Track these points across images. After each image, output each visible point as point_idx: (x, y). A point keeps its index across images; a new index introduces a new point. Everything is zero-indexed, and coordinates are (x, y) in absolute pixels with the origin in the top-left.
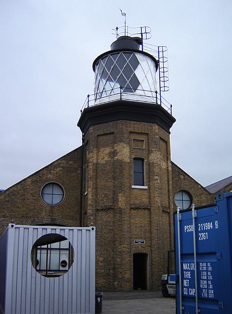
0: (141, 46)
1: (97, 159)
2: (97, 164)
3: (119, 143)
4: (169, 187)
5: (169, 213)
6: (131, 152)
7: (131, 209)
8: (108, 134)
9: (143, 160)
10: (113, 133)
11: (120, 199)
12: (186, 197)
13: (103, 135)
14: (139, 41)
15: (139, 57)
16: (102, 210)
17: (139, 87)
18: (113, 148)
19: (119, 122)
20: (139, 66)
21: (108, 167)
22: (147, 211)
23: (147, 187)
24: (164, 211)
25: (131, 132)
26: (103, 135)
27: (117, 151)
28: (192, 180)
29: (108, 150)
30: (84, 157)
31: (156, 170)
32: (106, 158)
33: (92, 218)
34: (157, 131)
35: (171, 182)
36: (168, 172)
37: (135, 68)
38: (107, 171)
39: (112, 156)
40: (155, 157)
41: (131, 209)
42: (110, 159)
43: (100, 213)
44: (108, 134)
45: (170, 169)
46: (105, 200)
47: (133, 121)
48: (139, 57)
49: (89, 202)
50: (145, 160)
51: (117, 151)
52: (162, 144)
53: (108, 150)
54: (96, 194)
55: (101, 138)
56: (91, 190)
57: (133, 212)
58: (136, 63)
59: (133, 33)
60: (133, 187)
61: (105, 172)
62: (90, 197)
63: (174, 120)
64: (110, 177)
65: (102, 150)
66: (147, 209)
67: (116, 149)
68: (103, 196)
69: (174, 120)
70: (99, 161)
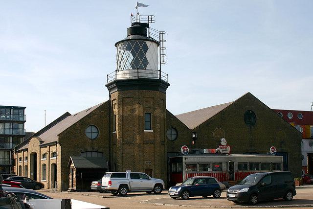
0: (148, 28)
5: (164, 145)
6: (144, 110)
9: (150, 114)
12: (174, 132)
14: (147, 25)
15: (148, 43)
29: (129, 108)
31: (158, 120)
32: (128, 113)
40: (158, 112)
45: (165, 117)
48: (148, 43)
50: (152, 114)
52: (162, 102)
53: (129, 108)
55: (125, 99)
57: (145, 145)
58: (146, 48)
59: (143, 21)
60: (145, 131)
63: (169, 85)
69: (169, 85)
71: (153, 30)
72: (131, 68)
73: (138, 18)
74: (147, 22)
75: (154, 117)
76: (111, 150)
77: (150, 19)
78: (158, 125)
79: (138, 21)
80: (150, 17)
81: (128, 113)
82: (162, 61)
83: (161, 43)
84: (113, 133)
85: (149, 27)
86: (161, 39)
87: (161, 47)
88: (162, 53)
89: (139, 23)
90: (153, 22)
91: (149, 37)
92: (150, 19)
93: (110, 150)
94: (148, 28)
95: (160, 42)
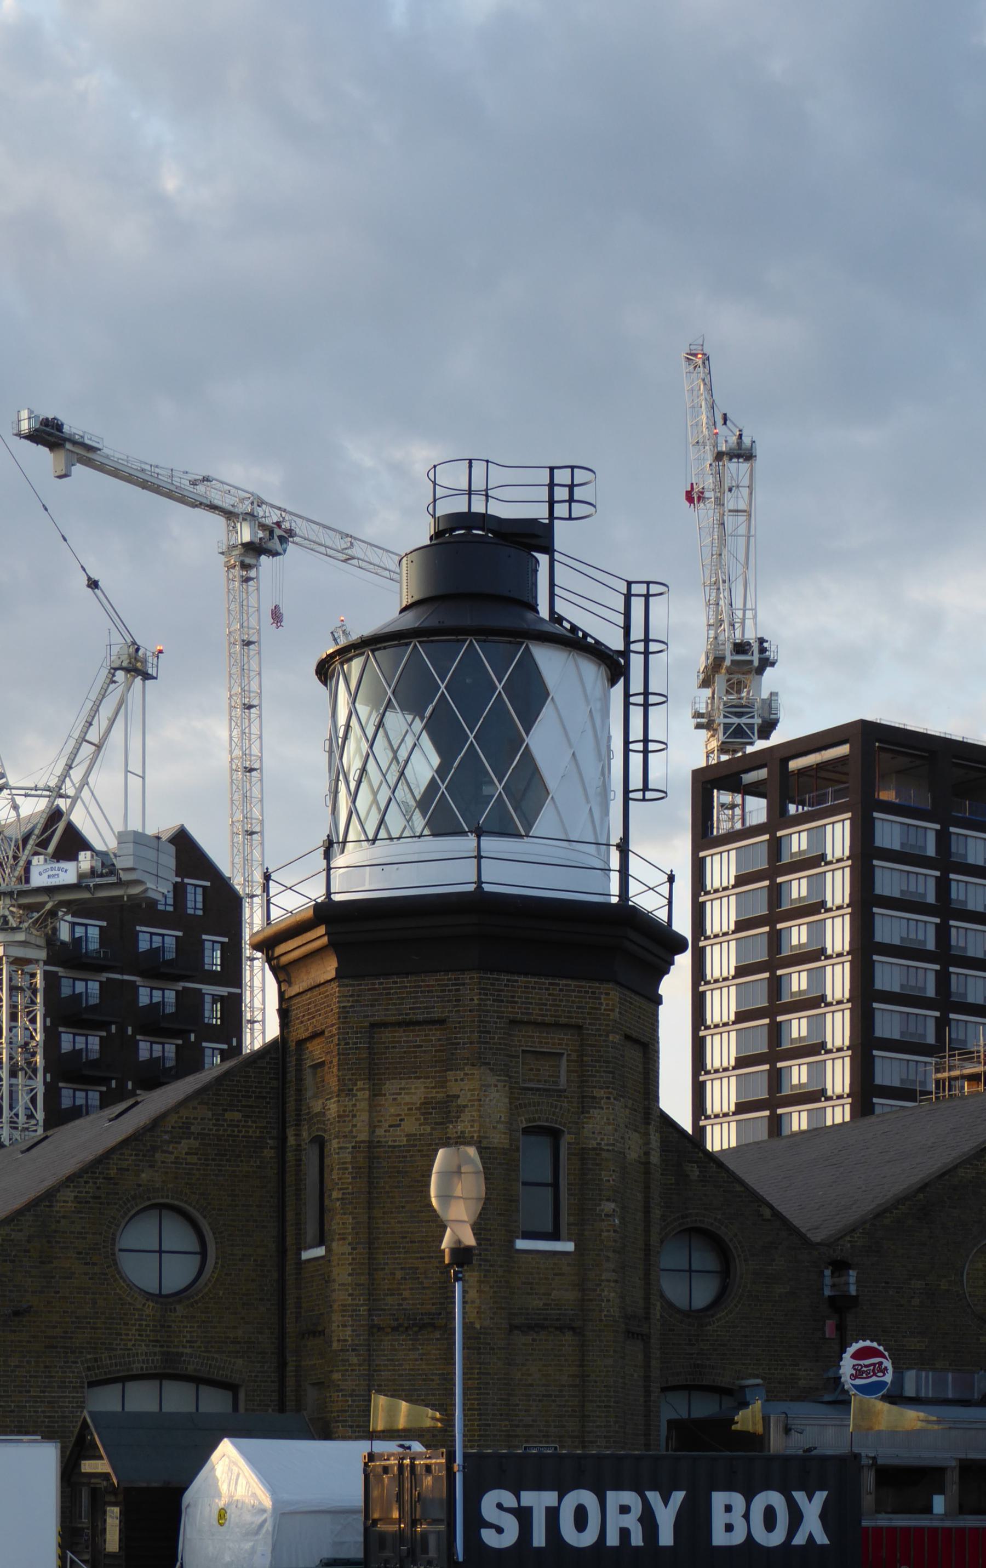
0: (543, 559)
1: (373, 1127)
2: (372, 1145)
3: (467, 1069)
4: (647, 1231)
5: (645, 1338)
7: (512, 1328)
8: (418, 1023)
9: (554, 1134)
10: (442, 1022)
13: (399, 1024)
17: (545, 823)
18: (443, 1084)
19: (466, 977)
20: (547, 712)
22: (568, 1337)
23: (569, 1246)
24: (630, 1334)
25: (513, 1022)
26: (399, 1024)
27: (460, 1102)
28: (739, 1188)
30: (291, 1092)
33: (354, 1360)
34: (615, 1015)
35: (656, 1213)
36: (647, 1173)
37: (530, 720)
41: (512, 1328)
42: (428, 1129)
44: (418, 1023)
45: (655, 1158)
46: (406, 1294)
47: (526, 974)
49: (340, 1296)
50: (566, 1139)
51: (460, 1102)
52: (633, 1055)
55: (386, 1036)
56: (347, 1249)
60: (521, 1244)
62: (342, 1274)
65: (391, 1086)
66: (573, 1329)
67: (454, 1089)
68: (399, 1275)
70: (380, 1132)
71: (582, 566)
72: (426, 832)
73: (478, 484)
74: (541, 512)
75: (582, 1154)
76: (291, 1368)
77: (561, 494)
78: (609, 1207)
79: (478, 506)
80: (562, 477)
82: (636, 781)
83: (636, 662)
84: (306, 1255)
85: (548, 549)
86: (637, 632)
87: (636, 686)
88: (636, 732)
89: (484, 520)
90: (578, 510)
91: (558, 619)
92: (561, 494)
93: (282, 1365)
94: (543, 559)
95: (626, 653)
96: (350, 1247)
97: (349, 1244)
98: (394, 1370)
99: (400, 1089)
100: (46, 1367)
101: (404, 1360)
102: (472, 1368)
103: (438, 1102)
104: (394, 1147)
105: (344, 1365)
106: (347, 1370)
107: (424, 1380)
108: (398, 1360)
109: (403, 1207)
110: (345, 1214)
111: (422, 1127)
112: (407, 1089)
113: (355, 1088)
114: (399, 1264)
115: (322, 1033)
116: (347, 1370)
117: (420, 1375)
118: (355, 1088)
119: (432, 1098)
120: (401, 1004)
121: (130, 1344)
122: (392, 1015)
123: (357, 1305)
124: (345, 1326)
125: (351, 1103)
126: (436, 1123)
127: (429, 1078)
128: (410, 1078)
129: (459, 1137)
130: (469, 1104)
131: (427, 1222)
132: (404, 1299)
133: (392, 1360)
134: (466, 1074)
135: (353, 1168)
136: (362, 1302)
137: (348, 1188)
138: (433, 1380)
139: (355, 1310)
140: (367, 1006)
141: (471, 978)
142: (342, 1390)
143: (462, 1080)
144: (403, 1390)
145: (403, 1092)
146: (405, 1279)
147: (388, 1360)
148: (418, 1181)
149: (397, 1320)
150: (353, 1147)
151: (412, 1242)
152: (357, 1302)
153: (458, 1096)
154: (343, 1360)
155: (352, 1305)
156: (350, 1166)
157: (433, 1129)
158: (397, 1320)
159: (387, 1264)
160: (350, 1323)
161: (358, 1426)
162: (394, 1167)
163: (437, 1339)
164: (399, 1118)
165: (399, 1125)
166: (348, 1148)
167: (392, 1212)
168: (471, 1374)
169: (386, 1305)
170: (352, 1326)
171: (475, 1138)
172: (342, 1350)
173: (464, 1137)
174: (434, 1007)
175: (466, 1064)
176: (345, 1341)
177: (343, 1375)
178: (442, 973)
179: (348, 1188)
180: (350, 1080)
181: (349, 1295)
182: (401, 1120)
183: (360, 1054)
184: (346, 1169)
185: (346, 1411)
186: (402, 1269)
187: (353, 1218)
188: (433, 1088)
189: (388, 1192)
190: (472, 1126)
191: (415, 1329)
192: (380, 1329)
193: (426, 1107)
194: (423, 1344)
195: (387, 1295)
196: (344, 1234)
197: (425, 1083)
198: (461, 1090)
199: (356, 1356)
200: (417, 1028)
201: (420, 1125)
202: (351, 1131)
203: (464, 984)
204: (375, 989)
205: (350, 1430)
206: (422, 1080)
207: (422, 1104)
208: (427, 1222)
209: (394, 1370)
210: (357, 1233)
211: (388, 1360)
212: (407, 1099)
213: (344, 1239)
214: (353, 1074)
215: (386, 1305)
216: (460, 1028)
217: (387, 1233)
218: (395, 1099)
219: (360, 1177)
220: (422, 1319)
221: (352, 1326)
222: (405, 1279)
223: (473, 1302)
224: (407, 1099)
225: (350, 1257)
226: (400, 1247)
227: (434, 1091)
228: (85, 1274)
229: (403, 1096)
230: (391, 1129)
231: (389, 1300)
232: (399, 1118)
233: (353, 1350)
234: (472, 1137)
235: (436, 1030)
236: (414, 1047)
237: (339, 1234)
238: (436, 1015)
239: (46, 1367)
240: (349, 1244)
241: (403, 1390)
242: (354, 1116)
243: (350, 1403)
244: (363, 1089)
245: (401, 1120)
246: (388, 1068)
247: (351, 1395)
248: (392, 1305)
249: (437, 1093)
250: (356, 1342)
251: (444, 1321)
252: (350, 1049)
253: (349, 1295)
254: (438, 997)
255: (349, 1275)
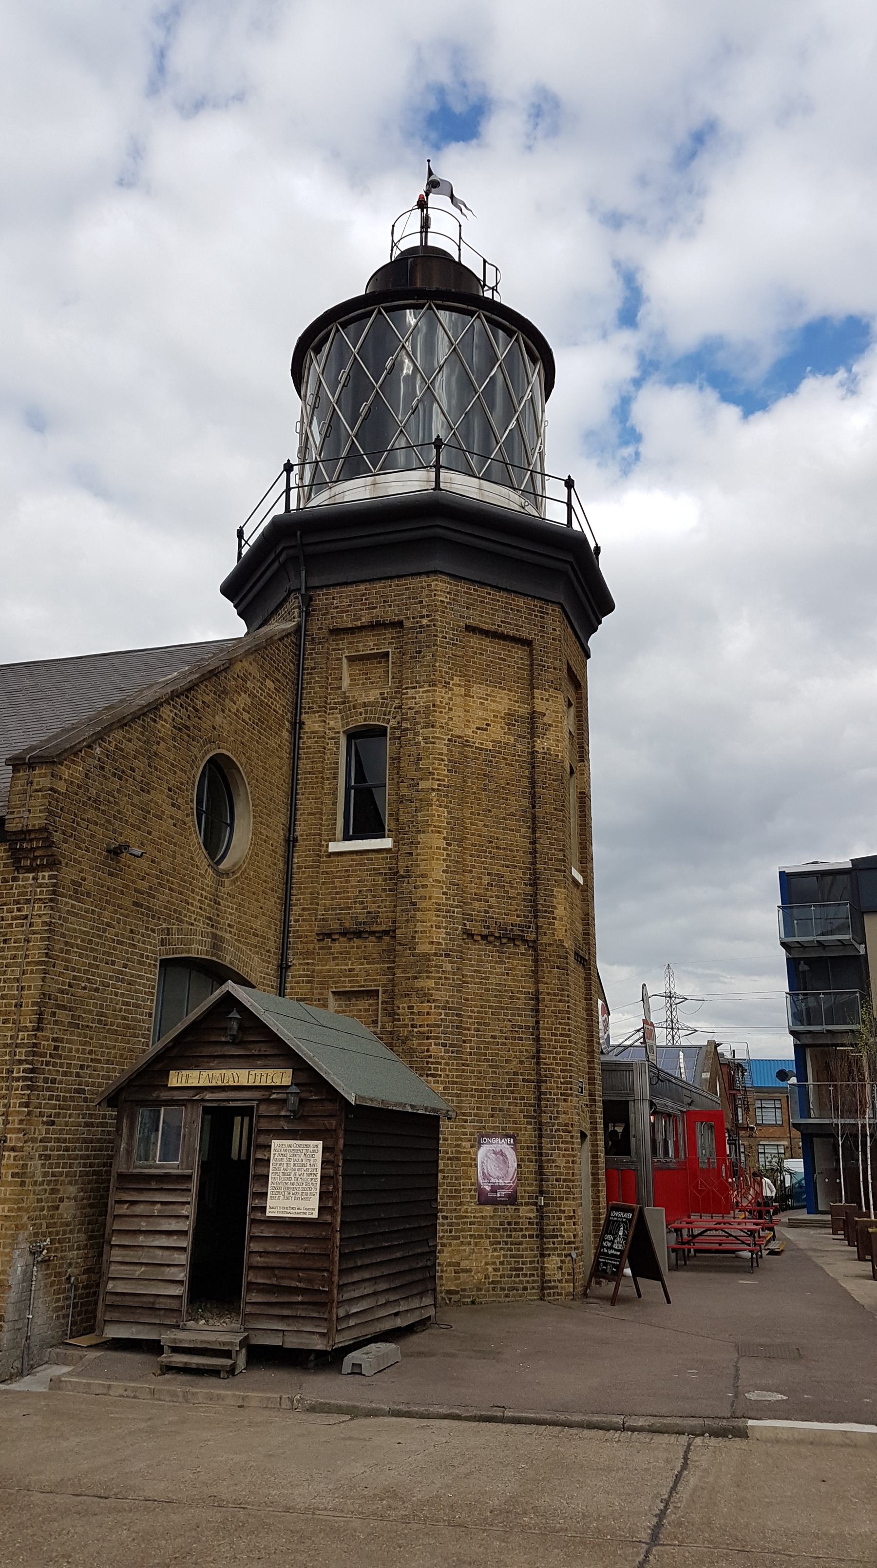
11: (560, 911)
13: (486, 633)
16: (484, 937)
21: (505, 770)
26: (486, 633)
27: (546, 720)
32: (497, 732)
33: (448, 967)
38: (503, 782)
39: (518, 728)
43: (474, 950)
46: (493, 901)
51: (546, 720)
54: (457, 866)
55: (475, 641)
61: (493, 786)
64: (513, 809)
68: (486, 879)
81: (497, 732)
84: (334, 847)
96: (445, 842)
97: (444, 838)
98: (481, 983)
99: (487, 695)
100: (132, 931)
101: (491, 973)
102: (563, 990)
103: (521, 717)
104: (482, 749)
105: (438, 972)
106: (440, 978)
107: (511, 998)
108: (485, 973)
109: (490, 811)
110: (440, 806)
111: (507, 736)
112: (493, 696)
113: (451, 682)
114: (485, 869)
115: (400, 624)
116: (440, 978)
117: (506, 991)
118: (451, 682)
119: (515, 711)
120: (494, 615)
121: (194, 916)
122: (486, 623)
123: (451, 906)
124: (438, 927)
125: (446, 696)
126: (519, 736)
127: (511, 691)
128: (496, 687)
129: (546, 753)
130: (554, 724)
131: (513, 830)
132: (490, 907)
133: (479, 972)
134: (550, 696)
135: (449, 761)
136: (456, 903)
137: (444, 780)
138: (518, 999)
139: (448, 911)
140: (464, 607)
141: (553, 610)
142: (434, 1001)
143: (547, 700)
144: (490, 1007)
145: (489, 698)
146: (492, 885)
147: (475, 971)
148: (503, 788)
149: (488, 927)
150: (449, 740)
151: (498, 848)
152: (452, 902)
153: (544, 715)
154: (436, 966)
155: (447, 905)
156: (446, 759)
157: (516, 740)
158: (488, 927)
159: (474, 867)
160: (444, 925)
161: (451, 1045)
162: (482, 769)
163: (522, 954)
164: (485, 722)
165: (486, 730)
166: (444, 740)
167: (479, 814)
168: (562, 995)
169: (474, 910)
170: (446, 928)
171: (560, 758)
172: (435, 954)
173: (550, 754)
174: (522, 627)
175: (550, 687)
176: (439, 944)
177: (436, 984)
178: (530, 598)
179: (444, 780)
180: (447, 673)
181: (444, 893)
182: (488, 725)
183: (456, 650)
184: (443, 760)
185: (439, 1026)
186: (489, 874)
187: (449, 813)
188: (515, 701)
189: (475, 793)
190: (557, 746)
191: (504, 941)
192: (471, 936)
193: (510, 718)
194: (509, 958)
195: (474, 899)
196: (439, 827)
197: (509, 695)
198: (547, 709)
199: (450, 962)
200: (502, 642)
201: (505, 733)
202: (447, 724)
203: (548, 614)
204: (471, 594)
205: (443, 1049)
206: (506, 692)
207: (506, 714)
208: (513, 830)
209: (481, 983)
210: (452, 829)
211: (475, 971)
212: (493, 706)
213: (439, 832)
214: (450, 668)
215: (474, 910)
216: (545, 652)
217: (473, 834)
218: (482, 703)
219: (455, 772)
220: (511, 930)
221: (446, 928)
222: (492, 885)
223: (561, 919)
224: (493, 706)
225: (445, 852)
226: (486, 852)
227: (517, 704)
228: (172, 817)
229: (489, 702)
230: (479, 731)
231: (476, 904)
232: (485, 722)
233: (447, 955)
234: (558, 756)
235: (518, 649)
236: (499, 659)
237: (435, 826)
238: (525, 634)
239: (132, 931)
240: (444, 838)
241: (490, 1007)
242: (450, 709)
243: (443, 1016)
244: (460, 685)
245: (488, 725)
246: (475, 672)
247: (444, 1008)
248: (479, 912)
249: (519, 707)
250: (450, 947)
251: (534, 935)
252: (448, 643)
253: (444, 893)
254: (526, 618)
255: (444, 871)
